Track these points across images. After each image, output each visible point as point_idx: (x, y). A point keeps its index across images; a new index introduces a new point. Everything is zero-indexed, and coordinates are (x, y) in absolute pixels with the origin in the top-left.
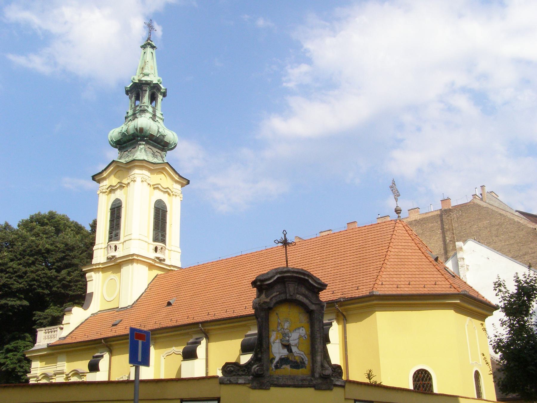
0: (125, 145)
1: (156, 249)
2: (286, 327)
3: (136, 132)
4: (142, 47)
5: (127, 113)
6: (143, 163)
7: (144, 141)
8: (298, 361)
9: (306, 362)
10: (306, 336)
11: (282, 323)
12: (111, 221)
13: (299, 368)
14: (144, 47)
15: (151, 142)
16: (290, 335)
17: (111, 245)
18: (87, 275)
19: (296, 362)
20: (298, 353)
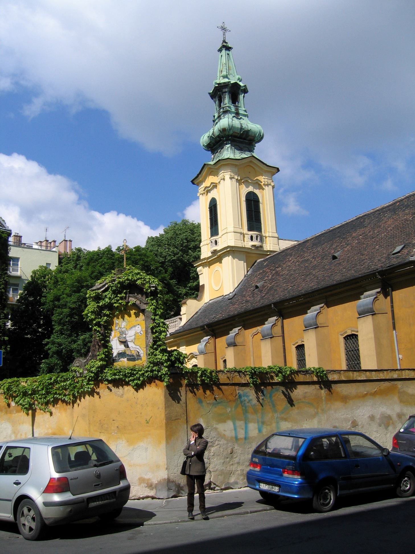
2: (123, 327)
5: (214, 116)
8: (134, 354)
9: (142, 355)
10: (142, 332)
11: (120, 324)
12: (211, 219)
13: (135, 361)
14: (220, 50)
16: (127, 333)
17: (212, 241)
18: (198, 269)
19: (133, 356)
20: (135, 348)
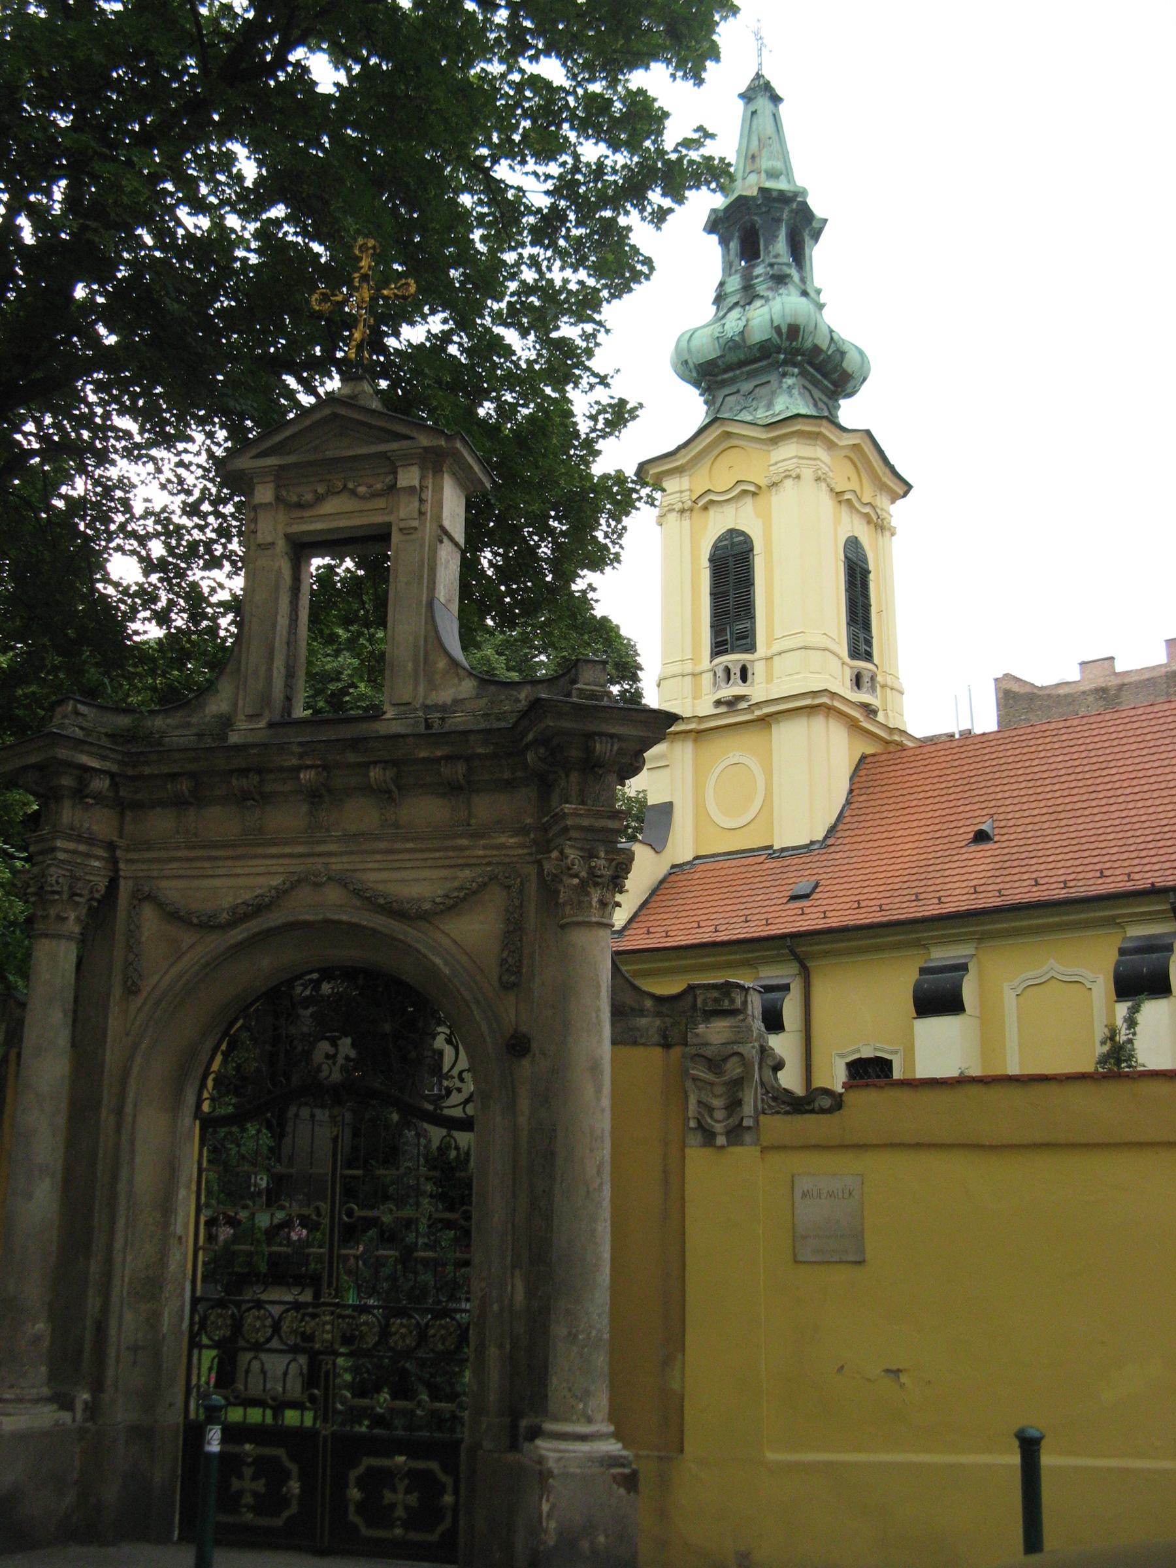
0: (730, 374)
1: (858, 681)
3: (775, 336)
4: (742, 96)
6: (820, 426)
7: (795, 365)
12: (717, 595)
15: (812, 370)
